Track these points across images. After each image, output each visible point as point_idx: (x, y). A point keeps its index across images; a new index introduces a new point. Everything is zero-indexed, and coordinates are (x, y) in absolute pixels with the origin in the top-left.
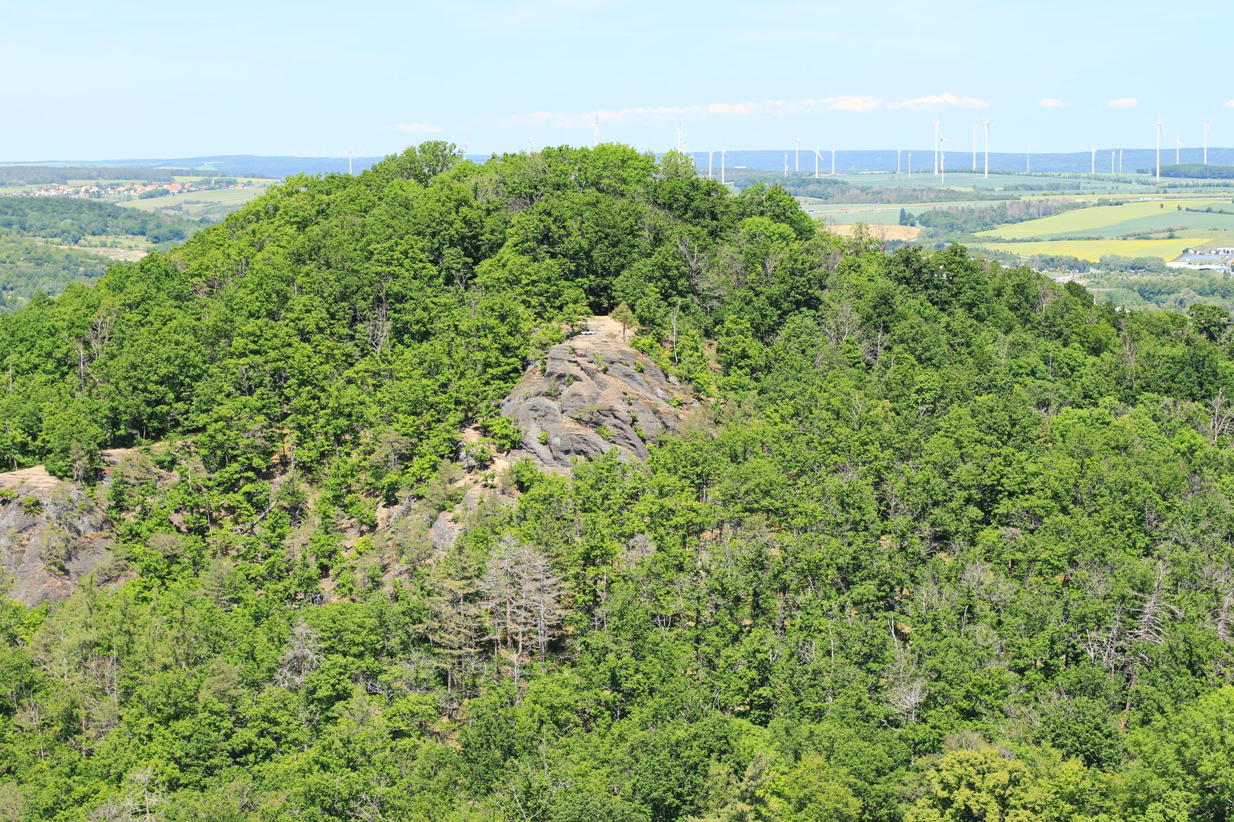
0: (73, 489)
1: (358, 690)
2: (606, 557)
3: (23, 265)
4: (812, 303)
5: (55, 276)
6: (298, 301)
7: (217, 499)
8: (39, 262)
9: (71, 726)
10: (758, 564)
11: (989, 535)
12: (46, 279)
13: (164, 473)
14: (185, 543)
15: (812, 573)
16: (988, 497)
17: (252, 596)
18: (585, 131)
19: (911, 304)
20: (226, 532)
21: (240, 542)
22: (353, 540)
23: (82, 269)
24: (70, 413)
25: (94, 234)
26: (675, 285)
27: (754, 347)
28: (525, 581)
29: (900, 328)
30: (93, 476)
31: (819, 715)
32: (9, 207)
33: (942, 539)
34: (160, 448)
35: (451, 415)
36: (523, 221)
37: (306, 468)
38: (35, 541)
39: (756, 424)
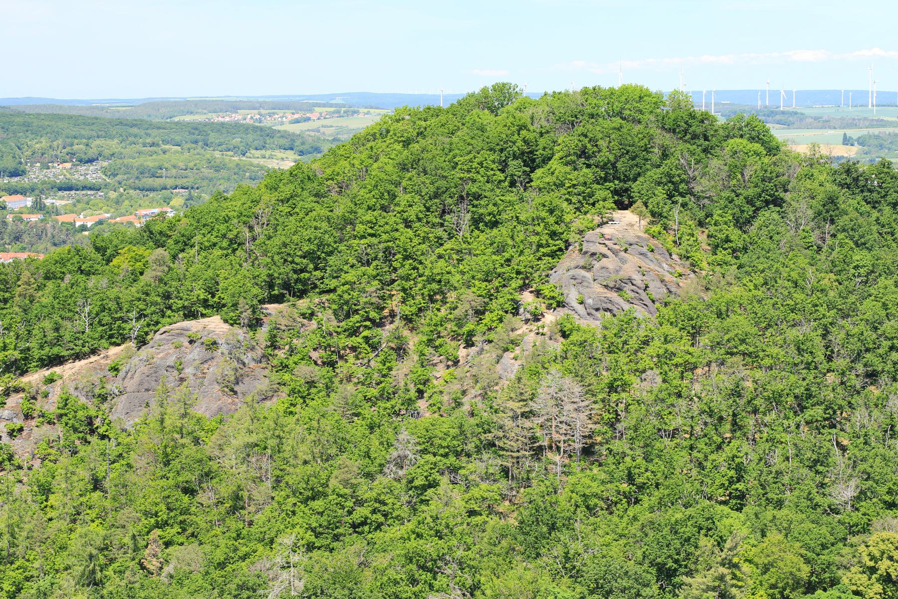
0: (241, 333)
1: (444, 480)
2: (625, 386)
3: (206, 172)
4: (778, 202)
5: (229, 179)
6: (403, 198)
7: (344, 341)
8: (217, 169)
9: (237, 504)
10: (736, 393)
12: (222, 181)
13: (309, 322)
14: (320, 373)
15: (776, 400)
17: (368, 411)
18: (612, 75)
19: (850, 203)
20: (350, 365)
21: (360, 372)
22: (441, 371)
23: (247, 174)
24: (238, 278)
25: (257, 149)
26: (676, 188)
27: (735, 234)
28: (566, 403)
29: (842, 221)
30: (255, 324)
31: (779, 504)
32: (196, 129)
33: (872, 376)
34: (303, 304)
35: (512, 282)
36: (567, 141)
37: (408, 319)
38: (214, 370)
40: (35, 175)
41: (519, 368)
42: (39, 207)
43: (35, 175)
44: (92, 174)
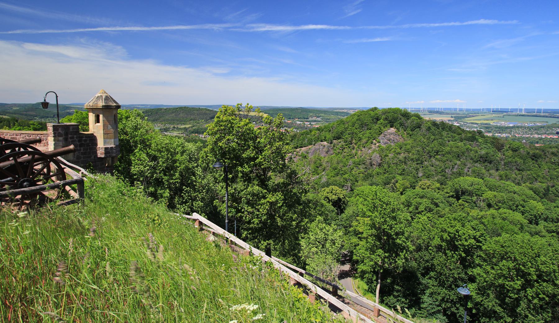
0: (329, 145)
2: (387, 156)
4: (419, 127)
6: (356, 125)
11: (438, 157)
13: (340, 143)
14: (341, 151)
15: (412, 159)
16: (437, 152)
17: (347, 157)
18: (390, 107)
19: (433, 128)
20: (345, 150)
22: (359, 152)
24: (329, 136)
26: (401, 124)
27: (411, 132)
30: (331, 143)
34: (339, 141)
35: (371, 139)
36: (384, 116)
38: (324, 150)
39: (409, 142)
40: (310, 119)
41: (371, 152)
42: (310, 124)
43: (310, 119)
44: (319, 119)
